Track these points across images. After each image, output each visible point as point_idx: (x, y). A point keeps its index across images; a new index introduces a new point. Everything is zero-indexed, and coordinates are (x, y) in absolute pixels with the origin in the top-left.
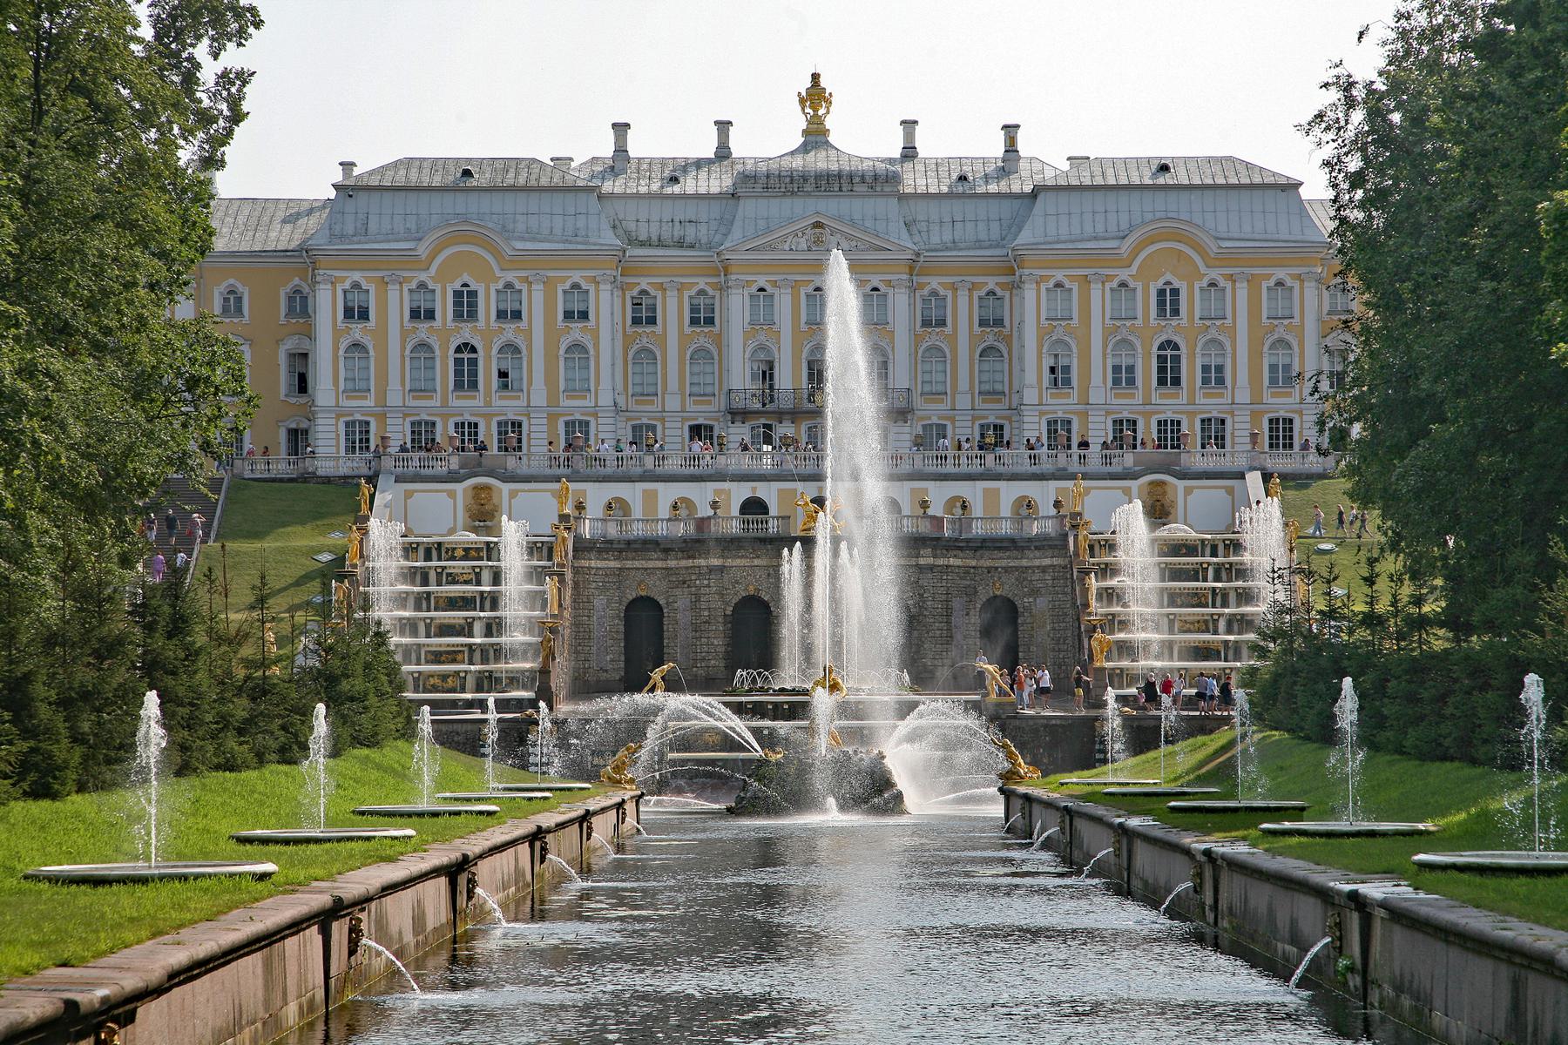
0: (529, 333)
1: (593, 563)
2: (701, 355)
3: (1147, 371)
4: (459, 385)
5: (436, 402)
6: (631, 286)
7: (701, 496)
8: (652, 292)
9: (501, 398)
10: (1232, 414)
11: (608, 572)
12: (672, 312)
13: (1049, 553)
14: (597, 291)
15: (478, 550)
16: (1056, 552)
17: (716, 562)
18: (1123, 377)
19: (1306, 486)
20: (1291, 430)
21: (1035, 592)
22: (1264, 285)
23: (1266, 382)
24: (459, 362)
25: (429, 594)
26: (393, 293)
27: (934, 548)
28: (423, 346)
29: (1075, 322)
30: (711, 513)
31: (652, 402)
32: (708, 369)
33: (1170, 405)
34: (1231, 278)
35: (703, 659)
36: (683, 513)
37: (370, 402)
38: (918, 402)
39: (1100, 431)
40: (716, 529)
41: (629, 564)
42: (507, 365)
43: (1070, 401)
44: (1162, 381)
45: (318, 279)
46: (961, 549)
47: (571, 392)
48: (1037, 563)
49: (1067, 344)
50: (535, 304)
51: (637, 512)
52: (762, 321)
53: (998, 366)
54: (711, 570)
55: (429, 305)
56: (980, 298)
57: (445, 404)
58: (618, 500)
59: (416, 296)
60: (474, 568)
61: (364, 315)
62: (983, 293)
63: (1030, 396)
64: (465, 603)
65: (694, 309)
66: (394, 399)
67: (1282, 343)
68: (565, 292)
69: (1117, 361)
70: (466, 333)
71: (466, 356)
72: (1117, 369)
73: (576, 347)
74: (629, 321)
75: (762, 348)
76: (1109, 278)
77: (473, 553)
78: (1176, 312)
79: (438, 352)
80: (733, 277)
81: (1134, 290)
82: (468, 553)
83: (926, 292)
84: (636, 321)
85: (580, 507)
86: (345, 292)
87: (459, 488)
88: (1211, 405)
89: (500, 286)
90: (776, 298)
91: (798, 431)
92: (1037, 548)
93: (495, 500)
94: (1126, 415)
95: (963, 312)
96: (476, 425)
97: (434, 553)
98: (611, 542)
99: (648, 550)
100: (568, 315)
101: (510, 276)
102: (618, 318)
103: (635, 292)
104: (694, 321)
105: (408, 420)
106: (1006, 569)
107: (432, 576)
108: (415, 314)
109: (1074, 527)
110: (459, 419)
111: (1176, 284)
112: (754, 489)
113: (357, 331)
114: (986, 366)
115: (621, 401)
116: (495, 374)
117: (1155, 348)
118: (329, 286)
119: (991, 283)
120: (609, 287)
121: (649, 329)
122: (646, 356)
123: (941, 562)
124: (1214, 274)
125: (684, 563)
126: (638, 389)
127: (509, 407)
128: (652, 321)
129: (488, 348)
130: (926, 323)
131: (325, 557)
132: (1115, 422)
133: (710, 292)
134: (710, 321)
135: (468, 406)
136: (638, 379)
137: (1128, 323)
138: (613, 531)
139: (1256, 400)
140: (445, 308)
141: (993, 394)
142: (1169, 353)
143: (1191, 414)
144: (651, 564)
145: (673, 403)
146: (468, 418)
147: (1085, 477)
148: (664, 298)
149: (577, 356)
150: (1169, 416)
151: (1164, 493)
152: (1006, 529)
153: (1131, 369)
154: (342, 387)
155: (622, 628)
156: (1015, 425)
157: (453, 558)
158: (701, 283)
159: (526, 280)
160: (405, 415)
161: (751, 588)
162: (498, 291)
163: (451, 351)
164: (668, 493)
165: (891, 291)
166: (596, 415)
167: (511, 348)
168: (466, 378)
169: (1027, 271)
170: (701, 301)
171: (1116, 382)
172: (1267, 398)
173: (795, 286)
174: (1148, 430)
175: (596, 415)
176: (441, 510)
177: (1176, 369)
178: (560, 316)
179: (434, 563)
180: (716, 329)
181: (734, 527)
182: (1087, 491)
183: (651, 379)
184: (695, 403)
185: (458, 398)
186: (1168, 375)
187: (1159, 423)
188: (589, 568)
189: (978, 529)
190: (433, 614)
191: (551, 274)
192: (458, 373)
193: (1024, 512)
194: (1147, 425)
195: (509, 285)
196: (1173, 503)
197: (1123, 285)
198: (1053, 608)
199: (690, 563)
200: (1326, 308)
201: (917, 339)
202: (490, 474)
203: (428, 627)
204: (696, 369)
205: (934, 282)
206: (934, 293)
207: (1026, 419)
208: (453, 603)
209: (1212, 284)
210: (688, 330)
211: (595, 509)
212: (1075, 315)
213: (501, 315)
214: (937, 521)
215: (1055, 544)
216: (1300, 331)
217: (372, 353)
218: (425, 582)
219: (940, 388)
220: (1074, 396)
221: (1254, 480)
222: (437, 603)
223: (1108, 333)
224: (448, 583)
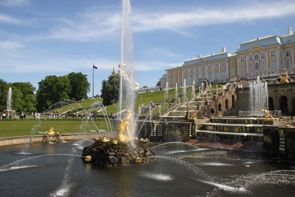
0: (265, 60)
4: (256, 69)
8: (289, 50)
24: (256, 65)
28: (251, 64)
70: (257, 61)
71: (257, 64)
84: (287, 56)
89: (261, 53)
100: (272, 56)
103: (286, 51)
121: (289, 56)
128: (289, 55)
148: (291, 51)
159: (264, 52)
163: (255, 64)
178: (270, 56)
191: (269, 50)
192: (256, 67)
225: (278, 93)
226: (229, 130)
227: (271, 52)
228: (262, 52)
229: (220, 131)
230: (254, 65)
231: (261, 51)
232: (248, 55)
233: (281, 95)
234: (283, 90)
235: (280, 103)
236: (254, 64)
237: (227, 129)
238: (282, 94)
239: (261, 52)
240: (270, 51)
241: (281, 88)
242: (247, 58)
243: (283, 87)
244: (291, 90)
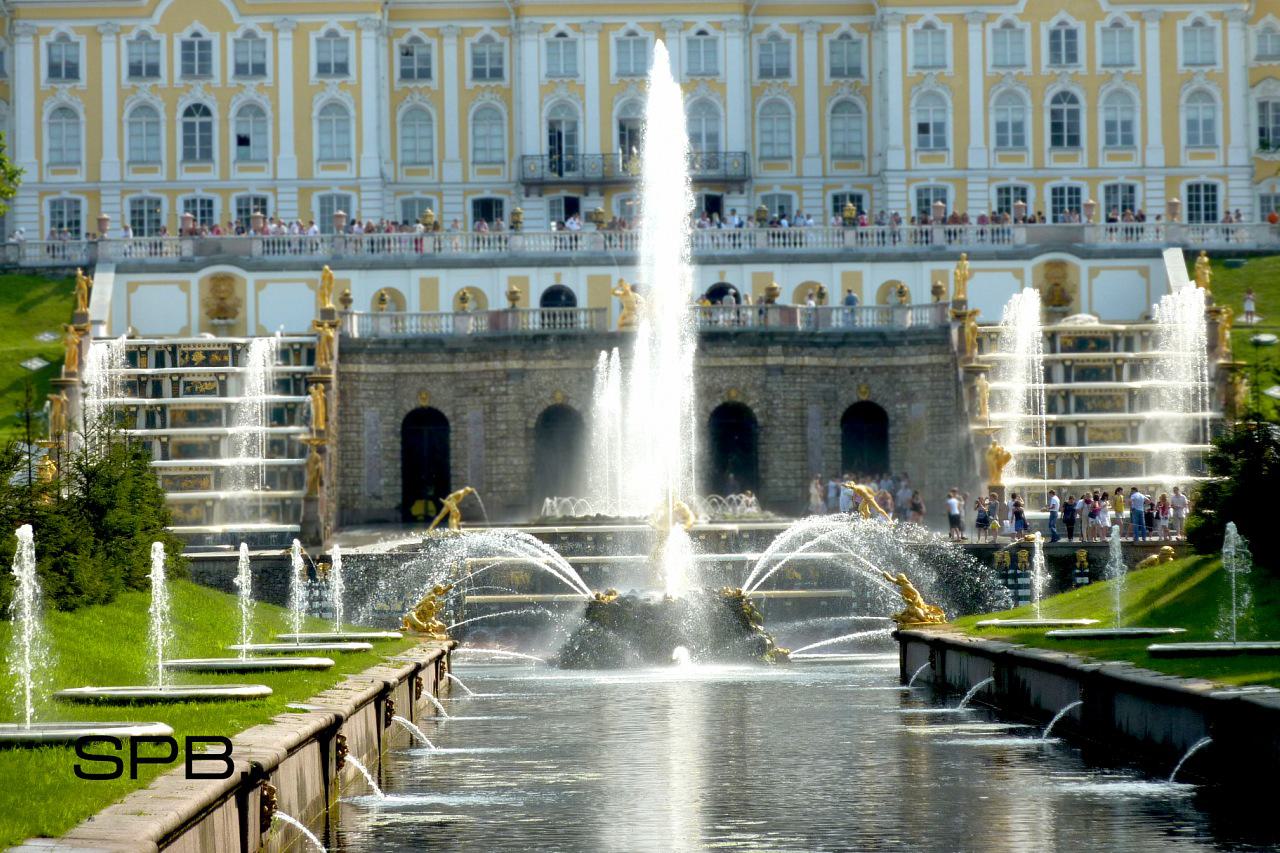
0: (274, 92)
1: (364, 368)
2: (486, 115)
3: (1038, 128)
4: (189, 155)
5: (162, 175)
6: (400, 33)
7: (494, 287)
8: (426, 39)
9: (241, 170)
10: (1143, 179)
11: (381, 379)
12: (451, 63)
13: (927, 348)
14: (359, 39)
15: (222, 353)
16: (936, 348)
17: (514, 364)
18: (1009, 136)
19: (1237, 265)
20: (1214, 198)
21: (909, 397)
22: (1180, 25)
23: (1183, 140)
24: (188, 127)
25: (163, 407)
26: (108, 48)
27: (785, 344)
28: (145, 109)
29: (950, 70)
30: (505, 304)
31: (426, 172)
32: (496, 131)
33: (1067, 169)
34: (1139, 17)
35: (500, 482)
36: (470, 306)
37: (80, 177)
38: (756, 168)
39: (981, 201)
40: (511, 326)
41: (406, 368)
42: (247, 130)
43: (944, 165)
44: (1057, 141)
45: (18, 30)
46: (817, 345)
47: (328, 162)
48: (912, 361)
49: (940, 99)
50: (282, 57)
51: (413, 305)
52: (561, 72)
53: (854, 124)
54: (509, 375)
55: (152, 60)
56: (832, 43)
57: (172, 178)
58: (393, 292)
59: (136, 49)
60: (217, 375)
61: (72, 72)
62: (835, 36)
63: (896, 160)
64: (210, 416)
65: (478, 59)
66: (110, 171)
67: (1202, 95)
68: (319, 41)
69: (1002, 117)
70: (198, 93)
71: (197, 120)
72: (1001, 127)
73: (333, 108)
74: (397, 74)
75: (563, 105)
77: (216, 357)
78: (1072, 57)
79: (163, 116)
80: (526, 20)
81: (1022, 31)
82: (210, 357)
83: (764, 35)
84: (406, 75)
85: (346, 300)
86: (50, 46)
87: (194, 279)
88: (1118, 169)
89: (239, 34)
90: (580, 44)
91: (607, 206)
92: (912, 343)
93: (238, 292)
94: (1013, 182)
95: (810, 59)
96: (210, 203)
97: (168, 358)
98: (383, 342)
99: (429, 351)
100: (323, 69)
101: (251, 23)
102: (384, 72)
103: (405, 40)
104: (478, 74)
105: (128, 197)
106: (874, 370)
107: (167, 386)
108: (135, 71)
109: (959, 317)
110: (189, 196)
111: (1073, 23)
112: (558, 276)
113: (65, 92)
114: (839, 125)
115: (389, 172)
116: (233, 141)
118: (30, 39)
119: (845, 24)
120: (372, 34)
121: (422, 84)
122: (418, 117)
123: (794, 361)
125: (475, 366)
126: (409, 157)
127: (251, 180)
128: (425, 74)
129: (225, 110)
130: (765, 73)
131: (36, 364)
132: (1000, 191)
133: (498, 38)
134: (497, 74)
135: (201, 180)
136: (409, 145)
137: (1015, 72)
138: (386, 328)
139: (1172, 162)
140: (171, 62)
141: (845, 158)
142: (1065, 107)
143: (1093, 181)
144: (434, 368)
145: (452, 173)
146: (200, 194)
147: (973, 256)
149: (334, 117)
150: (1066, 182)
151: (1065, 276)
152: (868, 320)
153: (1019, 127)
154: (46, 159)
155: (398, 446)
156: (877, 195)
157: (191, 364)
158: (486, 27)
159: (271, 27)
160: (123, 193)
161: (559, 398)
162: (236, 41)
163: (180, 114)
164: (450, 283)
165: (721, 35)
166: (358, 190)
167: (253, 110)
168: (198, 146)
169: (890, 10)
170: (487, 49)
171: (1001, 142)
172: (1185, 159)
173: (603, 30)
174: (1040, 200)
175: (358, 190)
176: (170, 308)
177: (1074, 126)
179: (168, 370)
180: (505, 83)
181: (533, 323)
182: (972, 272)
183: (425, 144)
184: (480, 172)
185: (188, 170)
186: (1064, 134)
187: (1054, 191)
188: (358, 374)
189: (837, 322)
190: (168, 431)
191: (301, 19)
192: (188, 140)
193: (894, 299)
194: (1039, 193)
195: (250, 34)
196: (1075, 288)
197: (1008, 25)
198: (933, 416)
199: (482, 366)
200: (1254, 52)
201: (754, 93)
202: (233, 261)
203: (164, 446)
204: (481, 131)
206: (775, 37)
207: (891, 188)
208: (193, 417)
209: (1117, 24)
210: (470, 84)
211: (361, 304)
212: (950, 60)
213: (241, 70)
214: (788, 313)
215: (935, 338)
216: (1223, 80)
217: (83, 118)
218: (157, 393)
219: (783, 151)
220: (949, 161)
221: (1174, 259)
222: (173, 417)
223: (990, 83)
224: (187, 393)
227: (319, 41)
228: (251, 23)
230: (171, 122)
231: (242, 15)
232: (128, 29)
236: (171, 110)
239: (237, 19)
240: (318, 26)
242: (113, 59)
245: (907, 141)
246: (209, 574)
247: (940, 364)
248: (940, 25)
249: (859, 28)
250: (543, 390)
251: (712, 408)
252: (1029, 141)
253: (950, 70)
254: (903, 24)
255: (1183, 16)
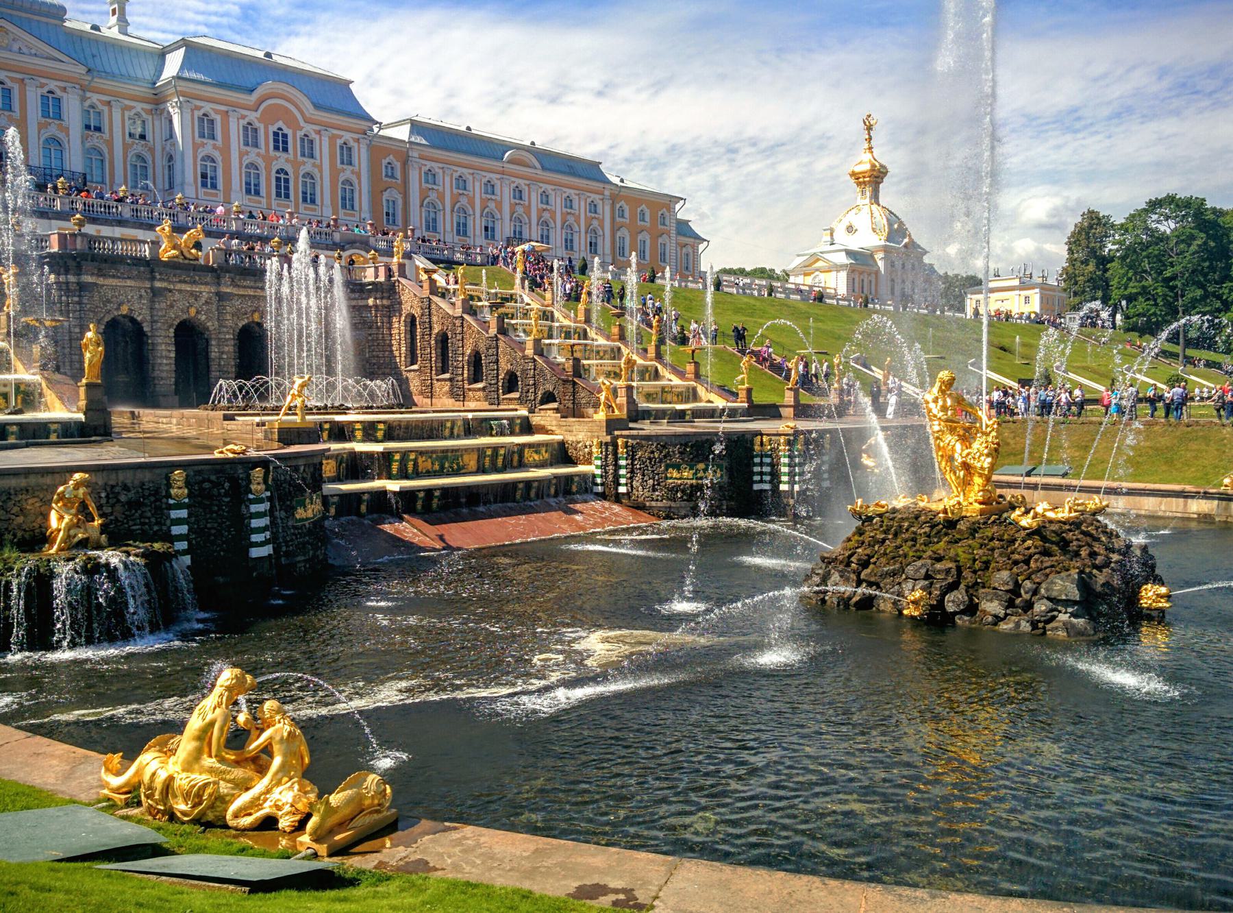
3: (267, 185)
17: (88, 279)
18: (252, 189)
34: (319, 132)
44: (278, 195)
72: (248, 184)
76: (243, 117)
78: (285, 150)
83: (87, 103)
111: (286, 130)
117: (274, 175)
124: (309, 128)
142: (282, 176)
161: (124, 310)
165: (65, 95)
171: (248, 192)
177: (287, 188)
205: (95, 98)
225: (172, 306)
226: (437, 467)
229: (404, 475)
233: (185, 317)
234: (192, 294)
235: (176, 351)
237: (428, 465)
238: (193, 311)
241: (185, 282)
243: (194, 282)
244: (228, 297)
245: (196, 182)
246: (126, 488)
247: (383, 306)
248: (213, 116)
249: (150, 112)
250: (109, 301)
251: (240, 325)
252: (263, 192)
253: (219, 143)
254: (192, 110)
255: (341, 137)
